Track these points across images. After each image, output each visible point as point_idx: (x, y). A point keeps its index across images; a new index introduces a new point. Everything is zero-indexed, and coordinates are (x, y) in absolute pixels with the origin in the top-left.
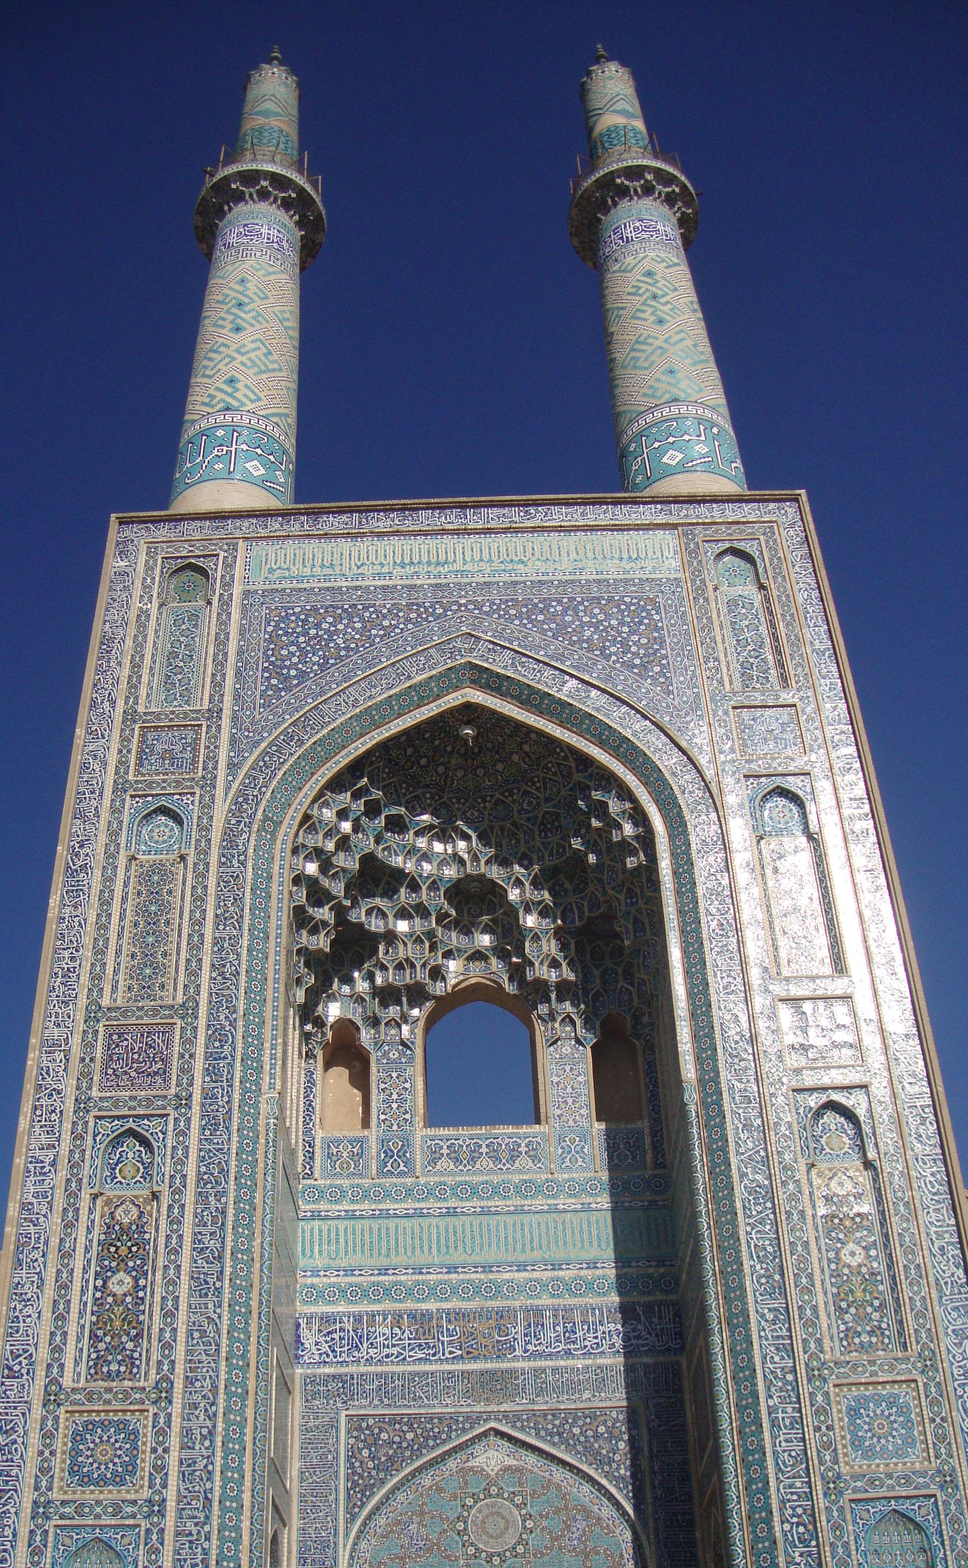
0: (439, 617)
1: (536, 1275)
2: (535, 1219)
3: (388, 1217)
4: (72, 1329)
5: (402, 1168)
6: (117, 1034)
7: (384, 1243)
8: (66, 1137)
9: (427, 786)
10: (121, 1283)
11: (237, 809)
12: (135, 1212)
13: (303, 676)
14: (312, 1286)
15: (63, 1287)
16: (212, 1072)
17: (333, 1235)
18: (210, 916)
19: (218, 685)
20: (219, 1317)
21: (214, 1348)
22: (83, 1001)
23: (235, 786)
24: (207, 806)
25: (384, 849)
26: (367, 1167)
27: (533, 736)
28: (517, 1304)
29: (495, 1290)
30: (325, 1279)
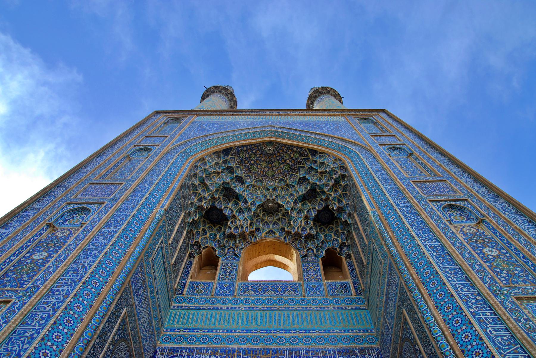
1: (295, 335)
2: (295, 313)
3: (218, 309)
5: (228, 293)
7: (213, 320)
9: (253, 173)
12: (68, 232)
14: (169, 335)
17: (186, 316)
20: (90, 266)
21: (79, 278)
25: (234, 187)
26: (211, 292)
27: (295, 149)
29: (273, 340)
30: (177, 333)
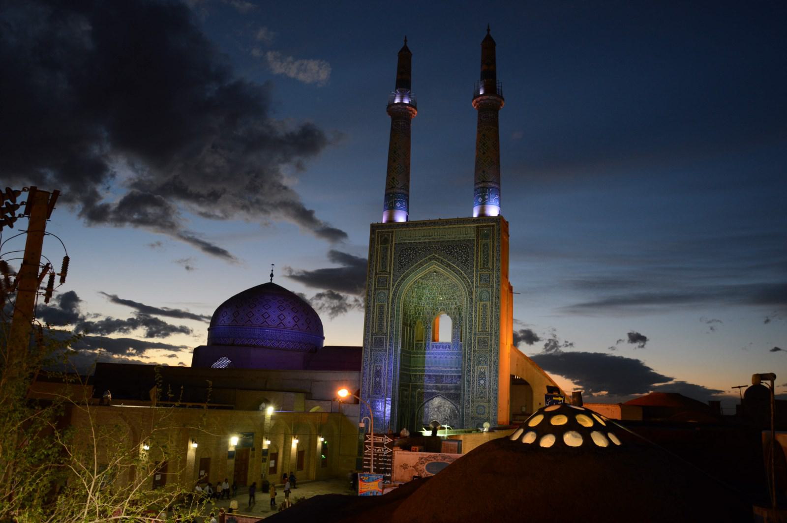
0: (429, 250)
4: (371, 386)
6: (376, 339)
8: (369, 356)
10: (378, 379)
11: (394, 295)
13: (405, 265)
15: (370, 380)
16: (390, 345)
18: (390, 317)
19: (390, 267)
22: (371, 332)
23: (394, 289)
24: (389, 294)
28: (444, 374)
29: (442, 371)
